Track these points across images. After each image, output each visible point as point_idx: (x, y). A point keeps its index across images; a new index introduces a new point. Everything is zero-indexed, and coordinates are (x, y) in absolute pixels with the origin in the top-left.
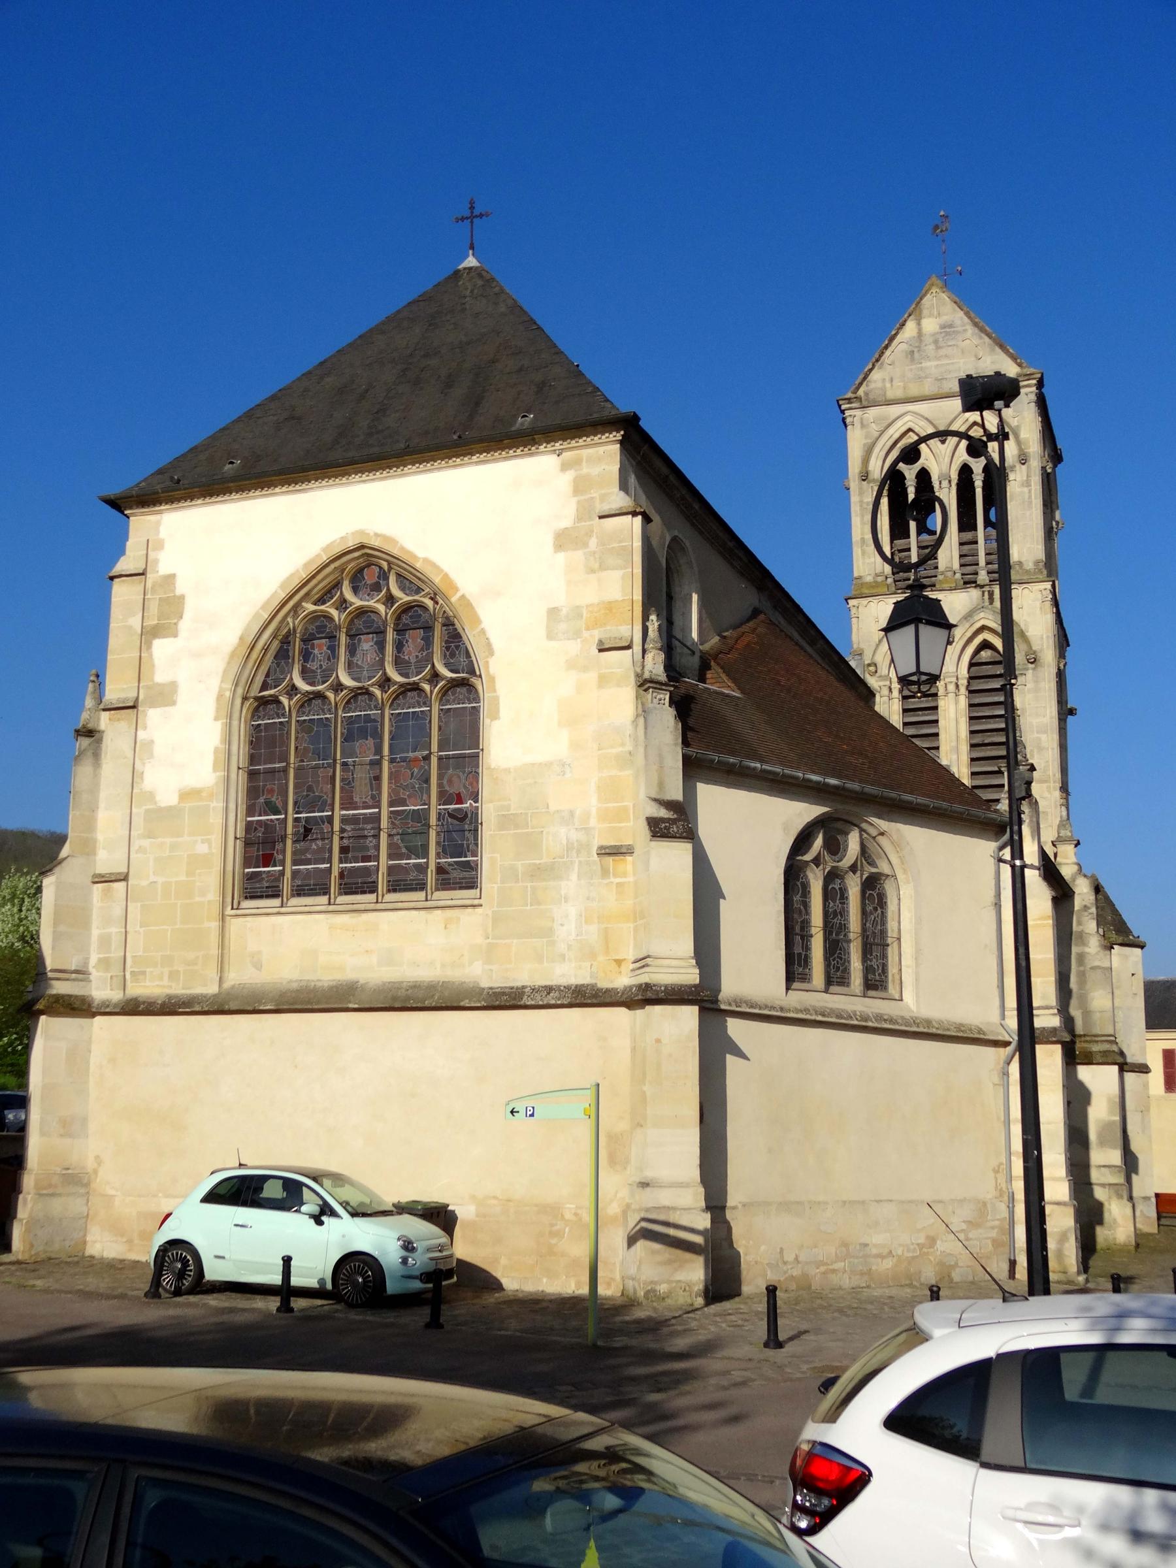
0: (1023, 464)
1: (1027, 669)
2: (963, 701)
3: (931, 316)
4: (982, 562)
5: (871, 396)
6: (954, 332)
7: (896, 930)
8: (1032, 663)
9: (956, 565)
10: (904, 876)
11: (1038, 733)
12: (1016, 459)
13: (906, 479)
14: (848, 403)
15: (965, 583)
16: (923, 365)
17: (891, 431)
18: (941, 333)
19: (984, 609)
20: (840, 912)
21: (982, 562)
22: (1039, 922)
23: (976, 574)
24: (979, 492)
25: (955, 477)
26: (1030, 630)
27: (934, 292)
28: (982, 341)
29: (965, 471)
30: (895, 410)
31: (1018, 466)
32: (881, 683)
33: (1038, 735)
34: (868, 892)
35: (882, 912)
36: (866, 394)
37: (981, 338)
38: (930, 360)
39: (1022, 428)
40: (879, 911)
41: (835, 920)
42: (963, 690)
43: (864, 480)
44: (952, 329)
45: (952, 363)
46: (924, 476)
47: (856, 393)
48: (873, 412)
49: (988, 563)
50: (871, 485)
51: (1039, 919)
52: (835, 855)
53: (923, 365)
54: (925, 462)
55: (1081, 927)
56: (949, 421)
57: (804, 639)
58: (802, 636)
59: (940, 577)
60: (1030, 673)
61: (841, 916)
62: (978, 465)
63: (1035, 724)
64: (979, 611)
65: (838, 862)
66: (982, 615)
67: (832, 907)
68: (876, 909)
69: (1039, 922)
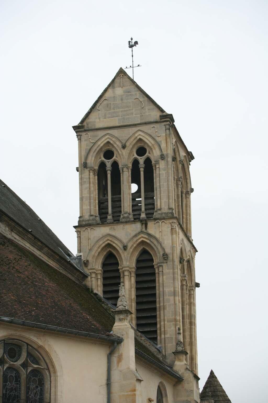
1: (163, 263)
2: (133, 280)
3: (120, 86)
4: (143, 209)
5: (90, 126)
6: (130, 95)
7: (49, 398)
8: (165, 260)
9: (131, 211)
10: (53, 369)
11: (169, 296)
12: (160, 157)
13: (106, 166)
14: (78, 129)
15: (135, 219)
17: (99, 143)
18: (124, 95)
20: (15, 389)
21: (143, 209)
22: (130, 393)
23: (140, 215)
24: (142, 173)
25: (130, 165)
26: (165, 243)
27: (121, 75)
28: (144, 99)
29: (136, 163)
30: (101, 133)
31: (160, 160)
32: (91, 271)
34: (33, 378)
35: (41, 389)
36: (88, 125)
37: (143, 98)
38: (119, 108)
39: (163, 142)
40: (39, 388)
41: (12, 393)
42: (133, 275)
43: (84, 167)
44: (130, 93)
45: (129, 110)
46: (115, 165)
47: (82, 124)
48: (90, 134)
49: (146, 210)
50: (88, 169)
51: (130, 391)
52: (13, 358)
53: (116, 110)
54: (116, 158)
56: (127, 138)
57: (34, 247)
58: (32, 245)
59: (122, 216)
60: (164, 265)
61: (16, 391)
62: (141, 160)
63: (167, 291)
65: (15, 362)
67: (11, 386)
68: (37, 387)
69: (130, 393)
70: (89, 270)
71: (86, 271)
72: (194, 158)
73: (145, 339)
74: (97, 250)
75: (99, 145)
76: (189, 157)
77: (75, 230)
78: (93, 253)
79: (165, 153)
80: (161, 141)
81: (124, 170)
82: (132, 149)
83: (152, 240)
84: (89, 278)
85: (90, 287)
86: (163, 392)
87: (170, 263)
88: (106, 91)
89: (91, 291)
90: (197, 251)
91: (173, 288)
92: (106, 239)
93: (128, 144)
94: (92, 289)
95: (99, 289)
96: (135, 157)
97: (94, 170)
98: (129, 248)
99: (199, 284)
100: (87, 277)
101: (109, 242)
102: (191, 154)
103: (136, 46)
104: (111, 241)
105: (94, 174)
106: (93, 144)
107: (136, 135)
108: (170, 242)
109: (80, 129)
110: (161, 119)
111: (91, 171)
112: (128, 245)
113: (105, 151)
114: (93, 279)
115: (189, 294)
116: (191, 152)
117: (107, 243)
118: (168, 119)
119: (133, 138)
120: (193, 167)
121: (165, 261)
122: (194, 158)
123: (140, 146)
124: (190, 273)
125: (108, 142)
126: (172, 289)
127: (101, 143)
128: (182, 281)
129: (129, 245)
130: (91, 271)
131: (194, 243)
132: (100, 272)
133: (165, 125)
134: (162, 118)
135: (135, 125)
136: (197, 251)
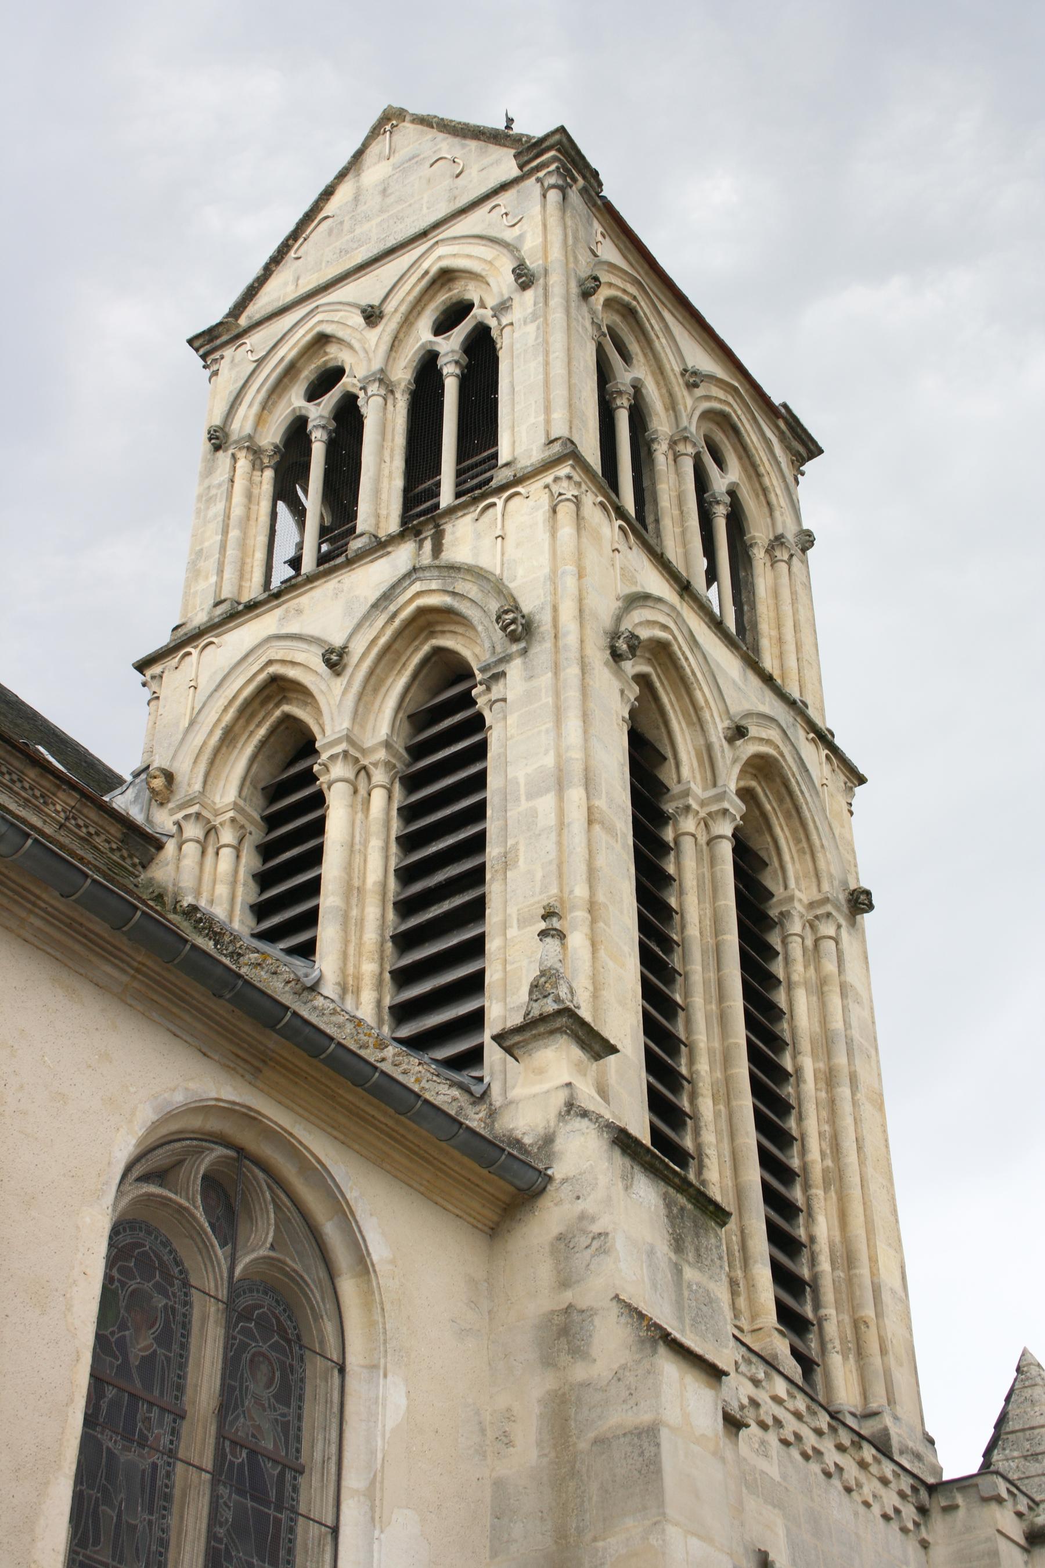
0: (524, 287)
1: (506, 659)
8: (514, 638)
16: (357, 232)
17: (281, 352)
19: (420, 574)
26: (520, 572)
31: (516, 297)
32: (179, 816)
33: (530, 804)
50: (230, 451)
55: (568, 1296)
60: (514, 669)
63: (522, 781)
64: (408, 582)
66: (417, 587)
70: (172, 812)
71: (163, 820)
72: (820, 451)
73: (398, 1055)
74: (219, 720)
75: (282, 359)
76: (782, 424)
77: (139, 677)
78: (197, 739)
79: (533, 264)
80: (521, 237)
81: (370, 393)
82: (408, 321)
83: (461, 587)
84: (170, 846)
85: (170, 888)
86: (330, 1230)
87: (542, 650)
88: (328, 193)
89: (168, 900)
90: (862, 780)
91: (552, 753)
92: (264, 660)
93: (389, 308)
94: (176, 895)
95: (222, 890)
96: (423, 346)
97: (255, 451)
98: (353, 658)
99: (868, 893)
100: (160, 847)
101: (272, 669)
102: (783, 411)
103: (510, 121)
104: (283, 662)
105: (257, 464)
106: (255, 364)
107: (425, 265)
108: (545, 559)
109: (217, 338)
110: (521, 167)
111: (242, 455)
112: (352, 646)
113: (312, 377)
114: (191, 849)
115: (809, 943)
116: (785, 406)
117: (262, 676)
118: (552, 153)
119: (413, 279)
120: (601, 177)
121: (515, 648)
122: (820, 451)
123: (448, 304)
124: (805, 844)
125: (322, 340)
126: (549, 761)
127: (288, 351)
128: (710, 822)
129: (357, 648)
130: (179, 816)
131: (838, 741)
132: (231, 814)
133: (538, 180)
134: (526, 158)
135: (424, 234)
136: (862, 780)
